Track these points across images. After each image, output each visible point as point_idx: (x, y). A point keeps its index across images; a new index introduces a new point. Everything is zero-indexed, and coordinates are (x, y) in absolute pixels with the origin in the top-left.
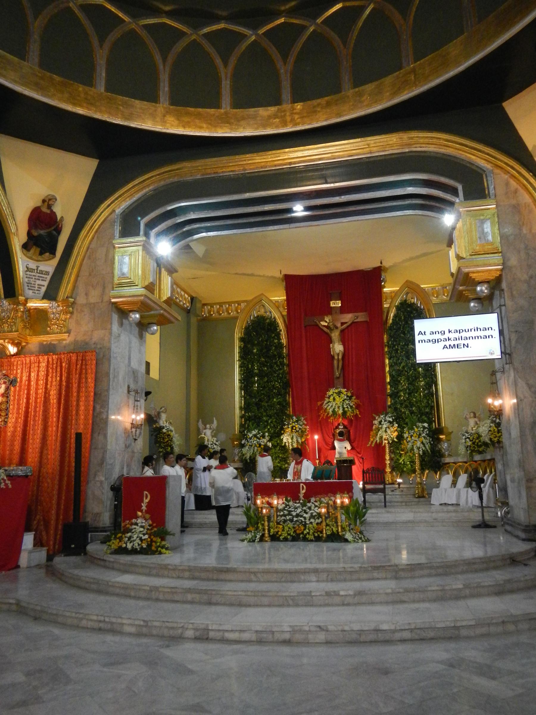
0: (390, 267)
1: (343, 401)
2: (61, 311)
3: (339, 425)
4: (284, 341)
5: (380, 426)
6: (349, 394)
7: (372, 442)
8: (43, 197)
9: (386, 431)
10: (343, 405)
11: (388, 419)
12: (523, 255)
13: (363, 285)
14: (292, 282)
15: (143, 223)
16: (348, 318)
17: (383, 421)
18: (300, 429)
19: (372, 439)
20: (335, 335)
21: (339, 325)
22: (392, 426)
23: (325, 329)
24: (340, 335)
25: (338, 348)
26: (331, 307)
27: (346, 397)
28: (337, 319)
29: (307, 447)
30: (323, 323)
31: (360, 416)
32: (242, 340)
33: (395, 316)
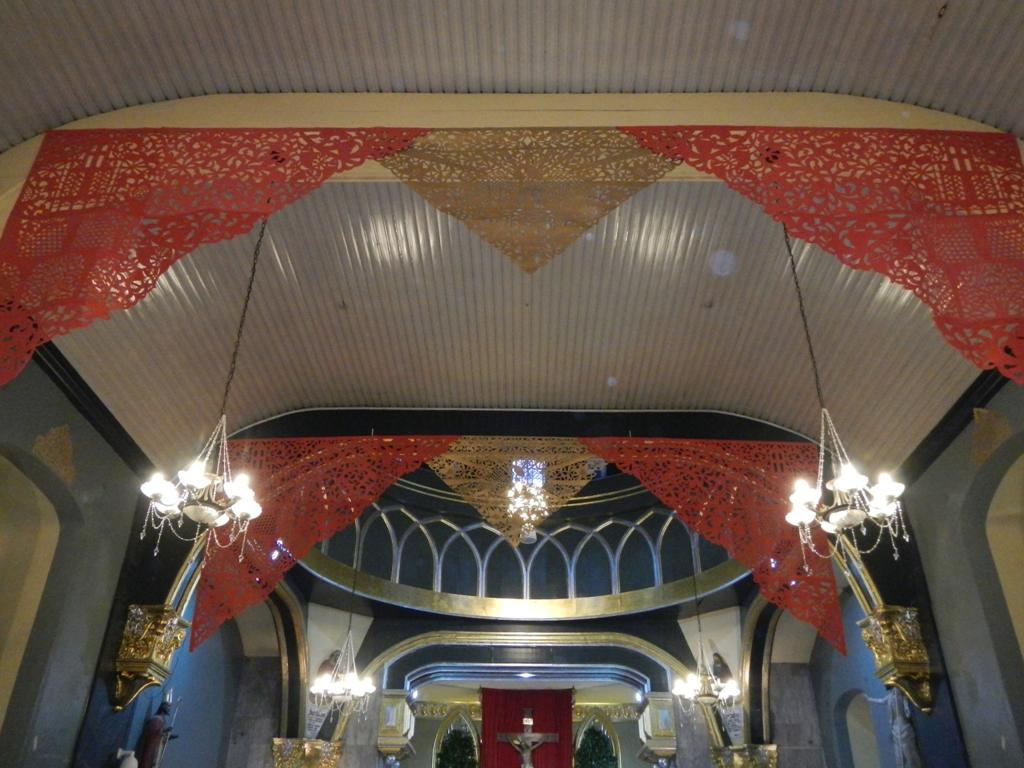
0: (581, 690)
2: (333, 751)
4: (477, 758)
8: (330, 653)
12: (691, 741)
13: (555, 706)
14: (487, 695)
15: (406, 677)
16: (537, 737)
20: (527, 756)
21: (530, 744)
23: (517, 748)
26: (524, 725)
28: (529, 732)
32: (438, 755)
33: (583, 740)
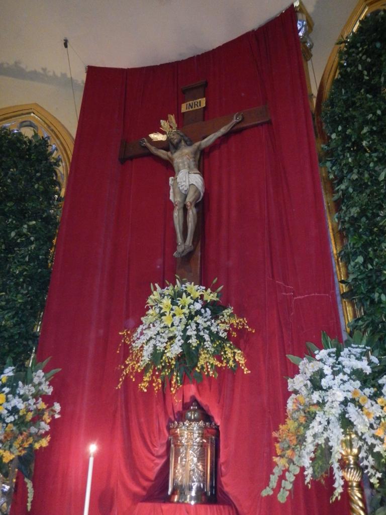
1: (191, 317)
3: (186, 407)
5: (316, 397)
6: (210, 296)
7: (282, 477)
9: (346, 423)
10: (185, 331)
11: (350, 362)
17: (327, 370)
18: (14, 411)
19: (281, 462)
20: (183, 158)
22: (374, 397)
23: (162, 153)
24: (195, 153)
25: (187, 180)
27: (198, 306)
29: (30, 485)
30: (157, 137)
31: (246, 371)
